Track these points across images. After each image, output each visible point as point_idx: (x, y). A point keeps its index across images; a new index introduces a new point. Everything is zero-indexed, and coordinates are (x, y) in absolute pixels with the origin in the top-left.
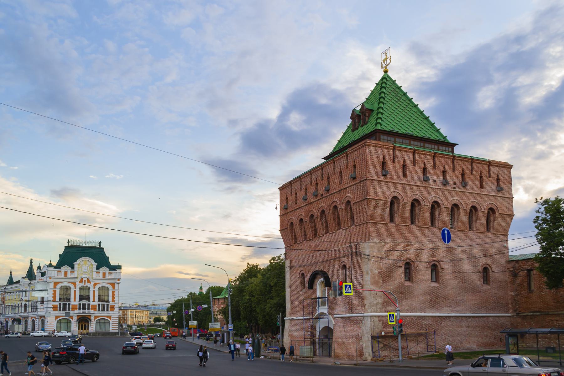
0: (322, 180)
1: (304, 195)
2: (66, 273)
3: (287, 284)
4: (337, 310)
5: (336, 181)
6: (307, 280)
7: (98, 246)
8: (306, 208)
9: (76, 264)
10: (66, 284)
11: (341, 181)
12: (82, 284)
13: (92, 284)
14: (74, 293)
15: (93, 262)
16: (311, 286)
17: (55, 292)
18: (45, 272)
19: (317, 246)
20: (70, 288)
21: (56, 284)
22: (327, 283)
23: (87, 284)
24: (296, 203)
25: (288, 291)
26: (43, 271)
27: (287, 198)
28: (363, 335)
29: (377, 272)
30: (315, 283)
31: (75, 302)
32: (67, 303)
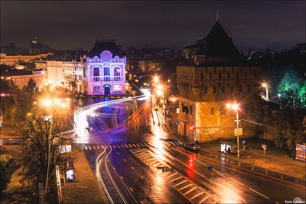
2: (96, 60)
7: (112, 42)
9: (101, 55)
10: (96, 67)
12: (106, 67)
13: (111, 66)
14: (102, 72)
15: (110, 52)
17: (91, 71)
18: (85, 59)
20: (98, 69)
21: (91, 67)
23: (108, 67)
26: (84, 58)
31: (102, 76)
32: (98, 77)
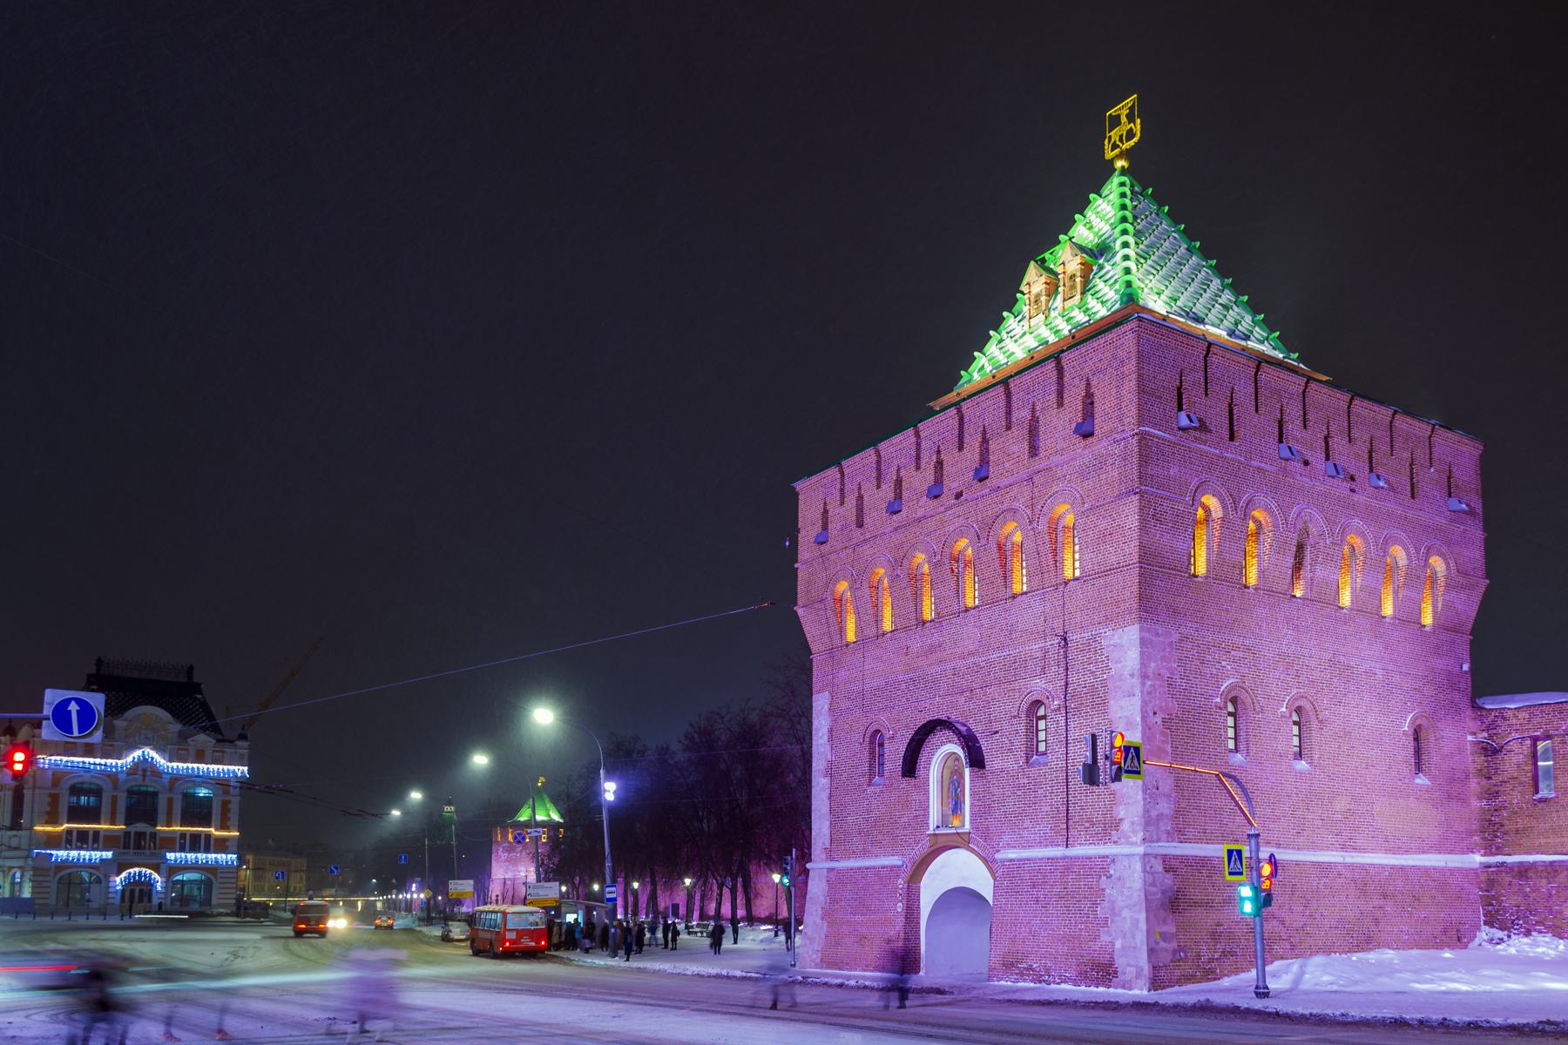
0: (961, 448)
1: (891, 496)
3: (818, 765)
4: (1006, 838)
5: (1015, 448)
6: (895, 752)
8: (898, 538)
11: (1034, 451)
16: (910, 766)
19: (932, 649)
22: (976, 759)
24: (860, 525)
25: (820, 786)
27: (826, 512)
28: (1114, 912)
29: (1159, 720)
30: (922, 759)
